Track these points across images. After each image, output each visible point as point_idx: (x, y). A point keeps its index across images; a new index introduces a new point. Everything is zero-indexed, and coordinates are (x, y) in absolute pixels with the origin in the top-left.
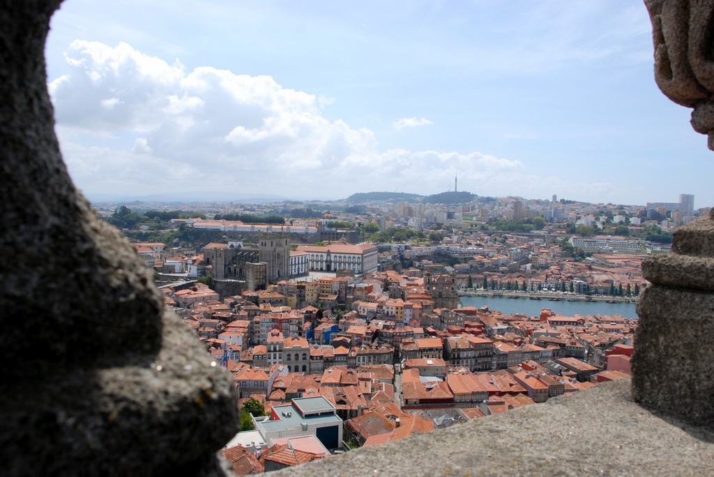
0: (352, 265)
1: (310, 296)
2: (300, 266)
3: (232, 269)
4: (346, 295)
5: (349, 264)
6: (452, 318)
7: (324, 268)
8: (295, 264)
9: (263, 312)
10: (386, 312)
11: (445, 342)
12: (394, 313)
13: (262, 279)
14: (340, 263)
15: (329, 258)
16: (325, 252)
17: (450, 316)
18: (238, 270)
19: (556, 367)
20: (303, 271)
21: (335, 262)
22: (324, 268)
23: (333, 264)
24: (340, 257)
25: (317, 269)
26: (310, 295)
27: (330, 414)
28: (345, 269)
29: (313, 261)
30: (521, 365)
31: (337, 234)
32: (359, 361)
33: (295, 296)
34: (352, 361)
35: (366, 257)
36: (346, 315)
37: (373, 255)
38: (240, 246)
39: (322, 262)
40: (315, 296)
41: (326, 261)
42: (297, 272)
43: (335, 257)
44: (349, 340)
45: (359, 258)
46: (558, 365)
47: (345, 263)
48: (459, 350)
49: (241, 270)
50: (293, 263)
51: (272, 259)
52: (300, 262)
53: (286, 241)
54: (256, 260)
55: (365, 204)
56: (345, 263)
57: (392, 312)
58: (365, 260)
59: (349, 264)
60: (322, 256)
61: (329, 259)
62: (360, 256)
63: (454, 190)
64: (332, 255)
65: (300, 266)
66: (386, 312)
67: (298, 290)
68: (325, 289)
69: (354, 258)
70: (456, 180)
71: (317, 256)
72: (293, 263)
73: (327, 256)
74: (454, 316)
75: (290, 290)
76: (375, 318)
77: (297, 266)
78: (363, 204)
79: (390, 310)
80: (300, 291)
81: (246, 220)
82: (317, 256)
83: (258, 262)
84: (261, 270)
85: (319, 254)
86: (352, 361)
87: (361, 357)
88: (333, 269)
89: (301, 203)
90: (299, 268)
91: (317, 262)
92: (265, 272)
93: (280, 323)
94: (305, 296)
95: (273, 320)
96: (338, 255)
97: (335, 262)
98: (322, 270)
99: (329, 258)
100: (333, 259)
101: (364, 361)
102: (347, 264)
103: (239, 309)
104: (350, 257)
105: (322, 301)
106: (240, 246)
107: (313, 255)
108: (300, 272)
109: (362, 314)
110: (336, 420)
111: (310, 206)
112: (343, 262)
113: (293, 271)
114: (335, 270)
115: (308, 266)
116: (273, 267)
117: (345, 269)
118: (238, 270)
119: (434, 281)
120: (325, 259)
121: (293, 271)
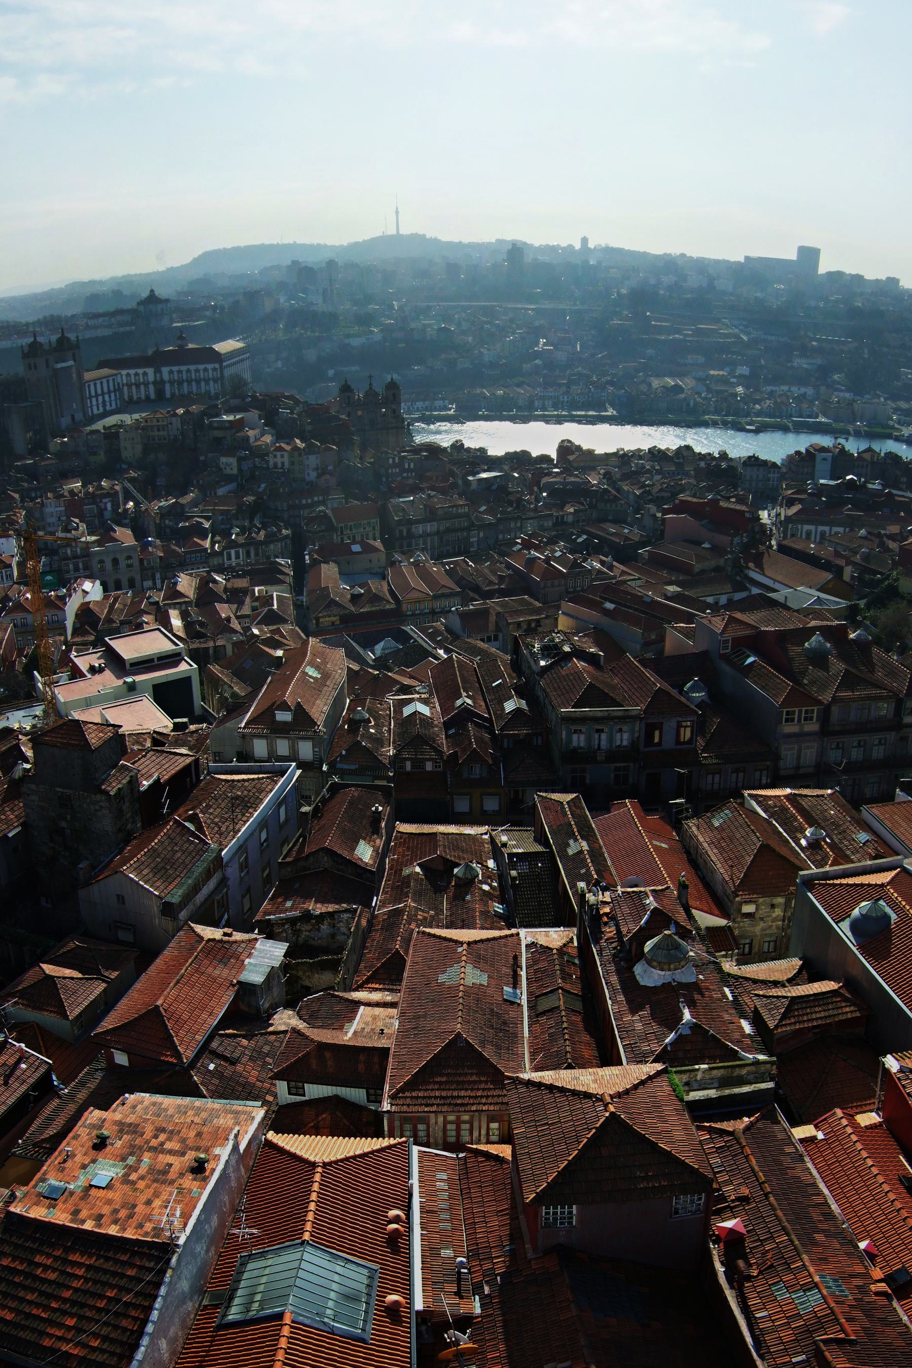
0: (203, 383)
1: (130, 450)
2: (107, 397)
5: (198, 382)
6: (394, 465)
7: (153, 396)
8: (97, 395)
10: (271, 464)
11: (383, 513)
12: (287, 465)
14: (180, 383)
15: (158, 375)
17: (391, 461)
19: (580, 540)
20: (114, 406)
21: (171, 383)
22: (153, 396)
23: (167, 386)
24: (180, 372)
27: (171, 660)
28: (190, 393)
29: (129, 385)
30: (519, 541)
32: (229, 558)
33: (102, 453)
34: (215, 561)
35: (229, 366)
37: (242, 360)
40: (139, 448)
42: (101, 410)
43: (171, 372)
44: (207, 525)
45: (215, 369)
46: (585, 537)
47: (189, 382)
48: (410, 522)
50: (93, 393)
52: (106, 390)
57: (283, 463)
60: (145, 374)
61: (158, 379)
62: (217, 366)
63: (392, 231)
65: (107, 397)
66: (271, 464)
68: (156, 433)
69: (206, 370)
70: (397, 212)
71: (136, 374)
72: (93, 393)
73: (155, 373)
74: (397, 460)
77: (100, 399)
79: (279, 460)
82: (136, 374)
85: (140, 371)
86: (215, 561)
87: (233, 552)
88: (168, 395)
91: (138, 386)
96: (175, 369)
97: (171, 383)
99: (158, 375)
100: (166, 377)
101: (237, 557)
102: (194, 384)
104: (197, 371)
107: (128, 375)
108: (108, 408)
109: (228, 471)
110: (185, 667)
113: (95, 408)
115: (122, 394)
117: (190, 393)
119: (359, 399)
120: (151, 378)
121: (95, 408)
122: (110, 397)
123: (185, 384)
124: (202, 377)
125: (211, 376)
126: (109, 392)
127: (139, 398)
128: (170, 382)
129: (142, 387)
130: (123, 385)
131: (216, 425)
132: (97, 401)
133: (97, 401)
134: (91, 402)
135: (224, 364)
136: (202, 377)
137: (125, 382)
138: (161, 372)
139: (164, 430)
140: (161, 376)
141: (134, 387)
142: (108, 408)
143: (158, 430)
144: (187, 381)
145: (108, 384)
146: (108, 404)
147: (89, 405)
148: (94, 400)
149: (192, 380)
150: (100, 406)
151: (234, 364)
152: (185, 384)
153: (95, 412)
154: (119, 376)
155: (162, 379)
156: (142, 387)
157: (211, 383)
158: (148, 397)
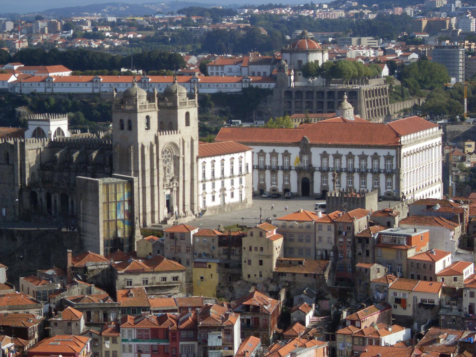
0: (369, 177)
2: (227, 182)
3: (42, 196)
4: (354, 262)
5: (363, 174)
9: (126, 311)
13: (123, 221)
16: (296, 144)
18: (56, 198)
20: (236, 199)
21: (324, 172)
22: (294, 188)
23: (317, 177)
24: (337, 156)
25: (274, 190)
26: (255, 262)
28: (350, 189)
31: (331, 93)
33: (214, 267)
36: (354, 317)
38: (59, 131)
39: (287, 170)
41: (299, 170)
43: (324, 155)
45: (388, 158)
47: (350, 173)
49: (64, 199)
50: (208, 176)
51: (148, 167)
52: (227, 173)
53: (187, 114)
54: (107, 170)
55: (409, 11)
56: (350, 173)
58: (405, 162)
59: (363, 174)
60: (286, 154)
62: (393, 152)
64: (316, 153)
65: (227, 182)
67: (221, 249)
69: (375, 157)
71: (274, 154)
72: (208, 176)
73: (302, 153)
75: (200, 251)
76: (435, 323)
77: (218, 184)
78: (399, 11)
80: (228, 253)
81: (80, 62)
82: (274, 154)
83: (111, 176)
84: (120, 197)
85: (280, 150)
89: (230, 12)
90: (223, 190)
91: (274, 171)
92: (131, 202)
93: (174, 339)
94: (240, 266)
95: (155, 334)
96: (331, 151)
97: (324, 172)
98: (286, 195)
100: (316, 162)
102: (356, 176)
103: (62, 305)
104: (363, 157)
105: (289, 278)
106: (59, 131)
107: (262, 154)
108: (228, 200)
109: (399, 311)
111: (253, 19)
112: (347, 171)
114: (323, 195)
116: (152, 186)
118: (56, 198)
122: (232, 184)
123: (344, 176)
124: (369, 167)
125: (382, 167)
126: (232, 176)
127: (274, 190)
128: (321, 170)
129: (280, 173)
130: (253, 168)
131: (386, 240)
132: (213, 186)
133: (213, 186)
134: (204, 188)
135: (404, 151)
136: (369, 167)
137: (256, 163)
138: (309, 154)
139: (308, 241)
140: (310, 160)
141: (268, 173)
142: (228, 200)
143: (301, 241)
144: (347, 171)
145: (232, 163)
146: (228, 193)
147: (201, 191)
148: (209, 185)
149: (354, 171)
150: (217, 195)
151: (418, 152)
152: (344, 176)
153: (209, 204)
154: (249, 153)
155: (310, 165)
156: (280, 173)
157: (382, 177)
158: (287, 190)
